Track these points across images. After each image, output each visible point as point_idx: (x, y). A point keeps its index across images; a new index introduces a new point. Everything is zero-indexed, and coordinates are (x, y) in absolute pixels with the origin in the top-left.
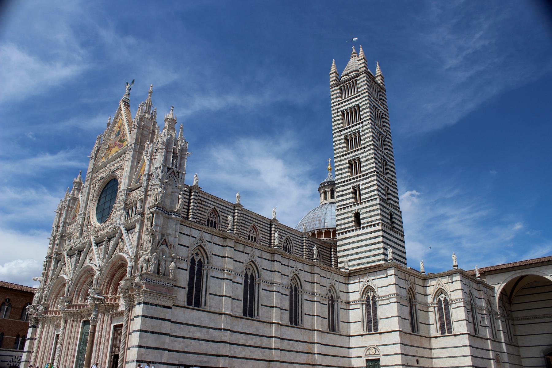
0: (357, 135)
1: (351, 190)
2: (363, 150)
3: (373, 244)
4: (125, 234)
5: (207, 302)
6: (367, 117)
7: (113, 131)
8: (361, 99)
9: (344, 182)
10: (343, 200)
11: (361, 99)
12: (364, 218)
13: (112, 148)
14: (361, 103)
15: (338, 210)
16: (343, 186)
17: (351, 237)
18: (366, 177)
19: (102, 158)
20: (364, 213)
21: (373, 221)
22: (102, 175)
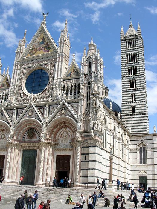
0: (135, 68)
1: (131, 95)
2: (138, 76)
3: (142, 123)
4: (67, 105)
5: (106, 146)
6: (141, 60)
7: (36, 40)
8: (138, 50)
9: (127, 90)
10: (125, 99)
11: (138, 50)
12: (138, 110)
13: (38, 50)
14: (138, 52)
15: (123, 104)
16: (126, 92)
17: (130, 118)
18: (139, 90)
19: (27, 54)
20: (138, 107)
21: (142, 112)
22: (30, 65)
